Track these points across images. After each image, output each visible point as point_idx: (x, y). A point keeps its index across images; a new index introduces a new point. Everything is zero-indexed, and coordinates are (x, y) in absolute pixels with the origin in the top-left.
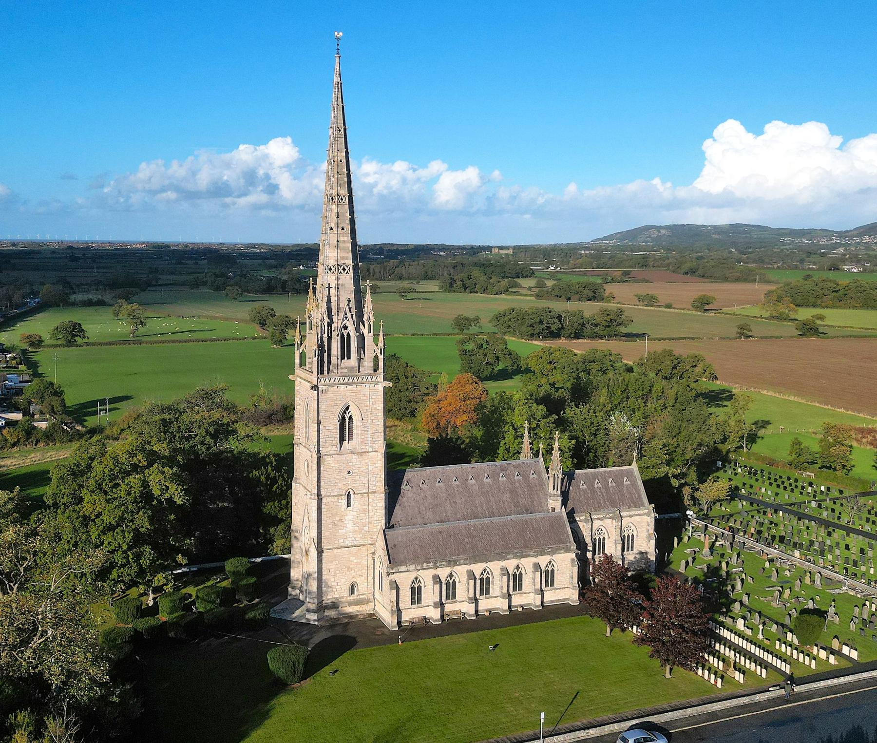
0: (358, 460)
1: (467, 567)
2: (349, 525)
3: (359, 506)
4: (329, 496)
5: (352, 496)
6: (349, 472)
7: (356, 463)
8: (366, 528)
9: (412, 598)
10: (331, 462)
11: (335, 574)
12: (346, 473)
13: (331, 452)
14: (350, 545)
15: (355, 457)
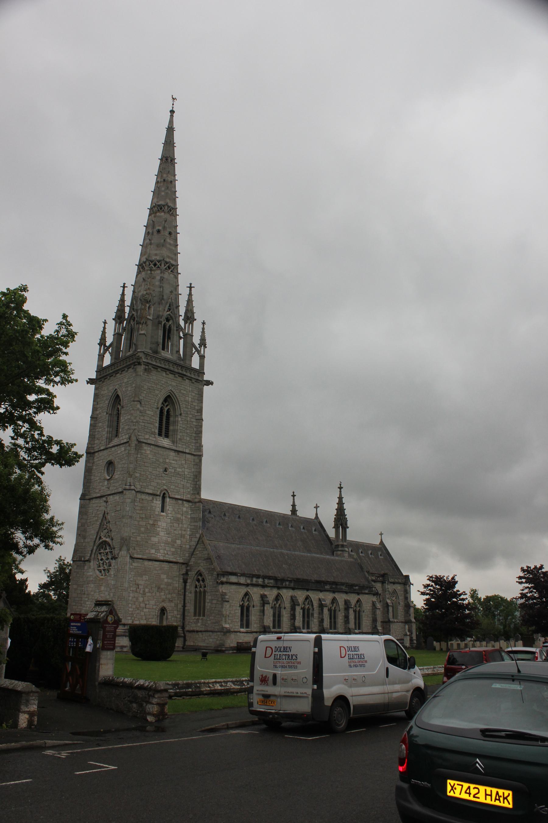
0: (176, 458)
1: (290, 593)
2: (162, 534)
3: (174, 513)
4: (143, 493)
5: (168, 500)
6: (166, 470)
7: (174, 462)
8: (179, 542)
9: (242, 620)
10: (148, 452)
11: (144, 594)
12: (162, 470)
13: (149, 442)
14: (161, 558)
15: (172, 454)
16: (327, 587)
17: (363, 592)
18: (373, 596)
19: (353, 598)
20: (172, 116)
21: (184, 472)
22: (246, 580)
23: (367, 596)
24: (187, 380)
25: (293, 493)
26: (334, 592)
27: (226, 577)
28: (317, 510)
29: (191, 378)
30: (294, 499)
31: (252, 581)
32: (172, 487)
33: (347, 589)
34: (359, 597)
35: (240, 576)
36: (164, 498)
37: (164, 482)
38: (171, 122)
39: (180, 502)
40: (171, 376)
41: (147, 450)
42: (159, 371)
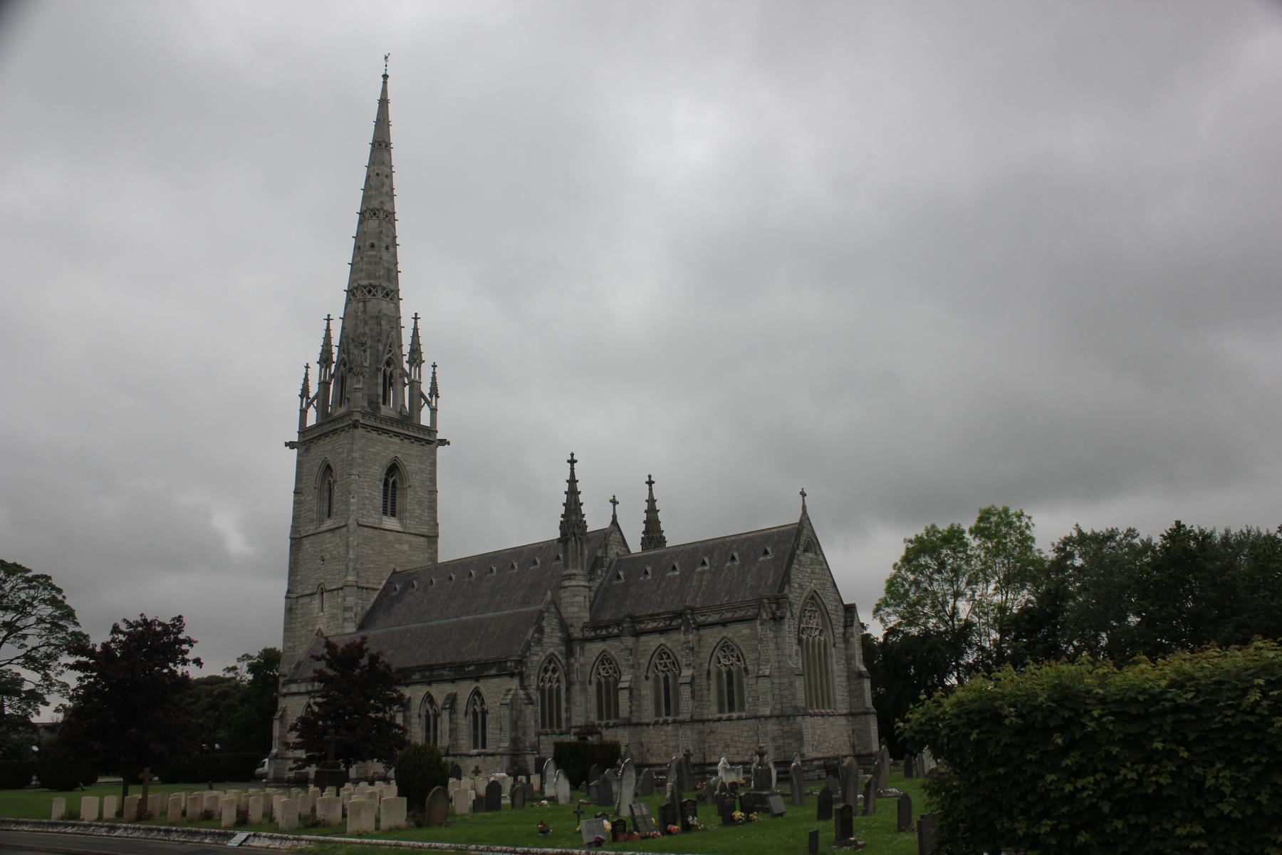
5: (324, 594)
7: (329, 546)
15: (328, 535)
16: (416, 677)
17: (485, 673)
18: (508, 679)
19: (464, 690)
20: (385, 83)
21: (339, 553)
22: (307, 687)
23: (496, 680)
24: (343, 432)
25: (650, 477)
26: (429, 683)
27: (287, 686)
28: (614, 508)
29: (342, 427)
30: (651, 490)
31: (313, 687)
32: (329, 577)
33: (452, 673)
34: (477, 684)
35: (300, 682)
36: (322, 593)
37: (321, 574)
38: (384, 91)
39: (335, 592)
40: (328, 439)
41: (306, 542)
42: (316, 443)
